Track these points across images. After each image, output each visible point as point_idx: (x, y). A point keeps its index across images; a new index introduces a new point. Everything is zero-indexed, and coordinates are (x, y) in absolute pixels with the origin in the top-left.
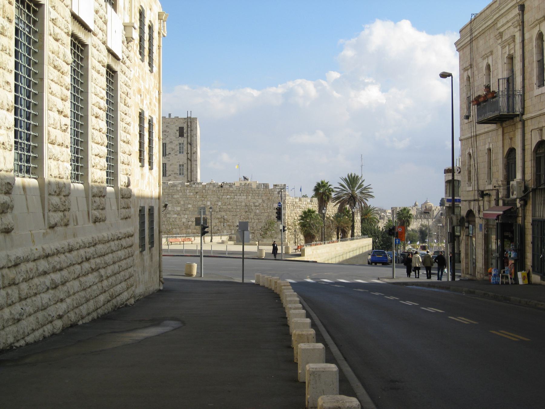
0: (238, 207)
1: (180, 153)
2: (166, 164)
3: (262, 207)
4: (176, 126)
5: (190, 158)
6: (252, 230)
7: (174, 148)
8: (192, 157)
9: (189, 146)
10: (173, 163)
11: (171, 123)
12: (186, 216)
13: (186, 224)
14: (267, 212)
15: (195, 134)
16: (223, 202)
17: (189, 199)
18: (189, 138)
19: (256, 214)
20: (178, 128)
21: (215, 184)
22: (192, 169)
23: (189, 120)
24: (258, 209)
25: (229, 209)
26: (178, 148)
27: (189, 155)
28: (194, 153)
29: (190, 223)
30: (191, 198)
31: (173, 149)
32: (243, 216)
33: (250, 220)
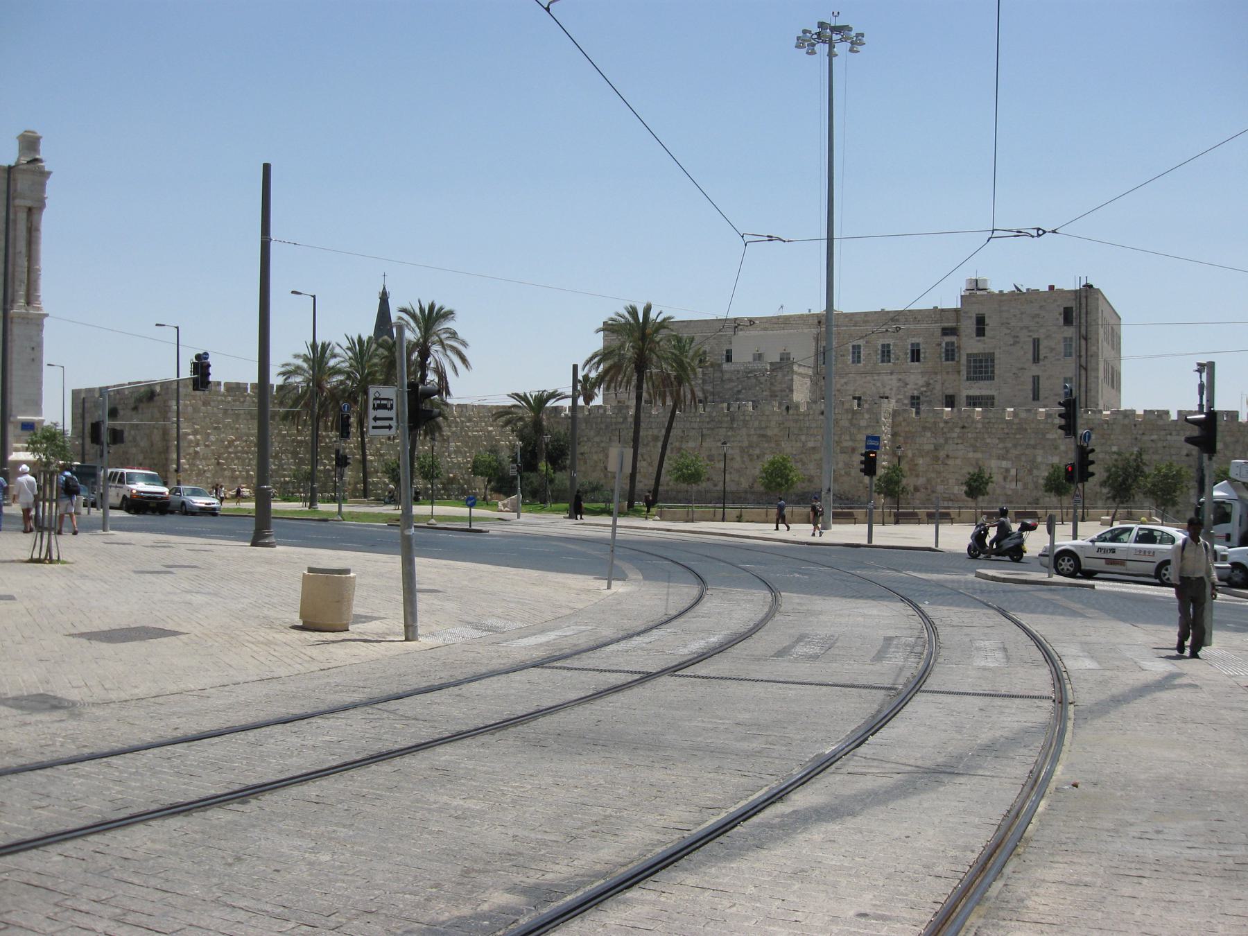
1: (1065, 356)
2: (1038, 377)
4: (1058, 306)
5: (1084, 364)
8: (1089, 365)
9: (1083, 342)
15: (1095, 320)
18: (1083, 329)
20: (1062, 309)
22: (1089, 386)
26: (1061, 347)
27: (1083, 359)
28: (1092, 356)
31: (1052, 350)
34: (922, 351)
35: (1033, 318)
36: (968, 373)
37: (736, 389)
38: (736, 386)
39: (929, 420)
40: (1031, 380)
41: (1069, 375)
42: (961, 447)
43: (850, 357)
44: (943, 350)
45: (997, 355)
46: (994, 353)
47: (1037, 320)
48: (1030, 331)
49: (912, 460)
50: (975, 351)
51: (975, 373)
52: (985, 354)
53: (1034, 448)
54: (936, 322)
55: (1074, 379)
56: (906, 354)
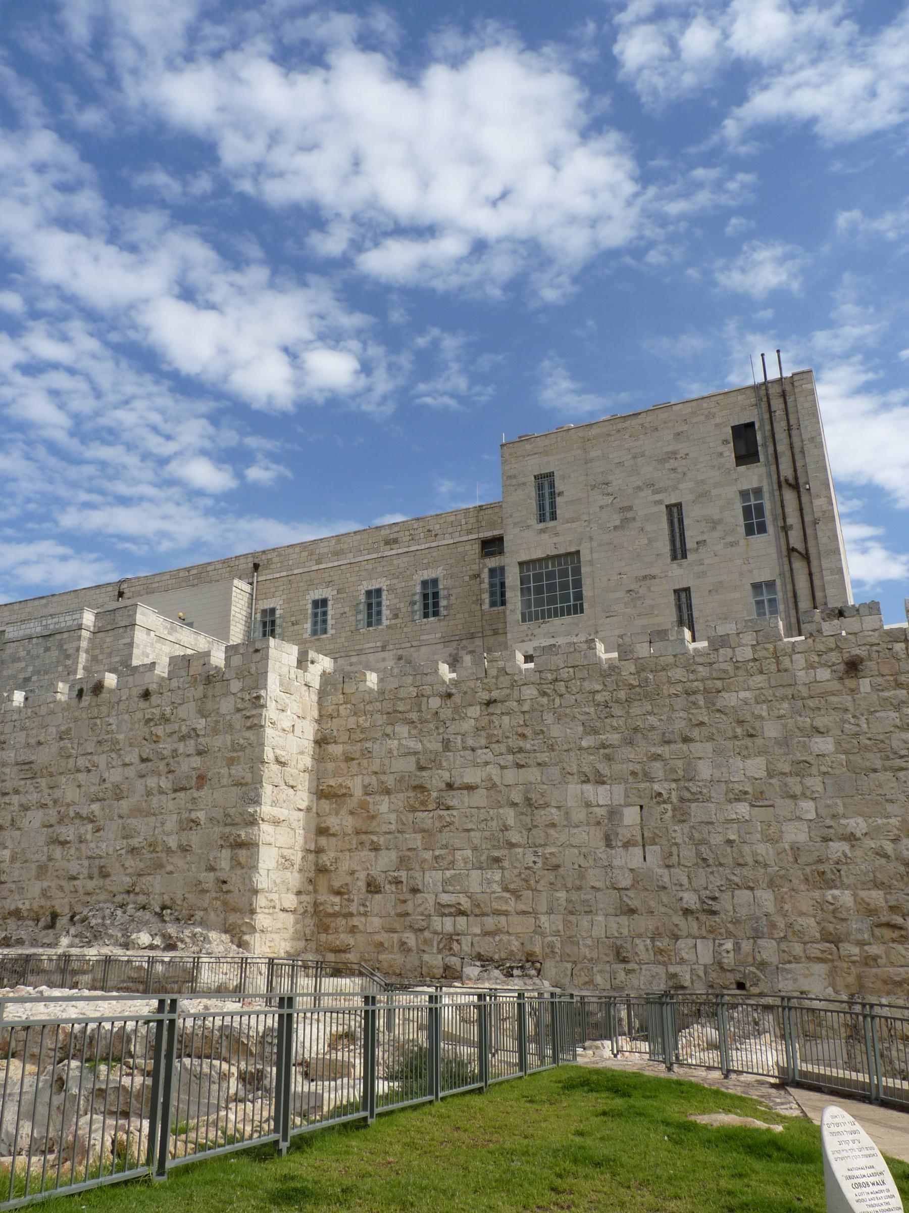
4: (717, 425)
5: (800, 546)
7: (716, 517)
8: (811, 543)
9: (789, 496)
10: (721, 582)
11: (695, 420)
12: (808, 808)
17: (811, 703)
22: (819, 595)
23: (774, 391)
29: (838, 848)
30: (822, 695)
31: (714, 524)
34: (442, 593)
35: (662, 461)
36: (527, 604)
37: (22, 676)
38: (23, 669)
39: (402, 693)
40: (672, 598)
41: (764, 576)
42: (483, 755)
43: (308, 626)
44: (486, 585)
45: (585, 556)
46: (578, 552)
47: (672, 464)
48: (657, 492)
49: (363, 805)
50: (538, 554)
51: (539, 603)
52: (559, 556)
53: (686, 740)
54: (469, 532)
56: (413, 603)
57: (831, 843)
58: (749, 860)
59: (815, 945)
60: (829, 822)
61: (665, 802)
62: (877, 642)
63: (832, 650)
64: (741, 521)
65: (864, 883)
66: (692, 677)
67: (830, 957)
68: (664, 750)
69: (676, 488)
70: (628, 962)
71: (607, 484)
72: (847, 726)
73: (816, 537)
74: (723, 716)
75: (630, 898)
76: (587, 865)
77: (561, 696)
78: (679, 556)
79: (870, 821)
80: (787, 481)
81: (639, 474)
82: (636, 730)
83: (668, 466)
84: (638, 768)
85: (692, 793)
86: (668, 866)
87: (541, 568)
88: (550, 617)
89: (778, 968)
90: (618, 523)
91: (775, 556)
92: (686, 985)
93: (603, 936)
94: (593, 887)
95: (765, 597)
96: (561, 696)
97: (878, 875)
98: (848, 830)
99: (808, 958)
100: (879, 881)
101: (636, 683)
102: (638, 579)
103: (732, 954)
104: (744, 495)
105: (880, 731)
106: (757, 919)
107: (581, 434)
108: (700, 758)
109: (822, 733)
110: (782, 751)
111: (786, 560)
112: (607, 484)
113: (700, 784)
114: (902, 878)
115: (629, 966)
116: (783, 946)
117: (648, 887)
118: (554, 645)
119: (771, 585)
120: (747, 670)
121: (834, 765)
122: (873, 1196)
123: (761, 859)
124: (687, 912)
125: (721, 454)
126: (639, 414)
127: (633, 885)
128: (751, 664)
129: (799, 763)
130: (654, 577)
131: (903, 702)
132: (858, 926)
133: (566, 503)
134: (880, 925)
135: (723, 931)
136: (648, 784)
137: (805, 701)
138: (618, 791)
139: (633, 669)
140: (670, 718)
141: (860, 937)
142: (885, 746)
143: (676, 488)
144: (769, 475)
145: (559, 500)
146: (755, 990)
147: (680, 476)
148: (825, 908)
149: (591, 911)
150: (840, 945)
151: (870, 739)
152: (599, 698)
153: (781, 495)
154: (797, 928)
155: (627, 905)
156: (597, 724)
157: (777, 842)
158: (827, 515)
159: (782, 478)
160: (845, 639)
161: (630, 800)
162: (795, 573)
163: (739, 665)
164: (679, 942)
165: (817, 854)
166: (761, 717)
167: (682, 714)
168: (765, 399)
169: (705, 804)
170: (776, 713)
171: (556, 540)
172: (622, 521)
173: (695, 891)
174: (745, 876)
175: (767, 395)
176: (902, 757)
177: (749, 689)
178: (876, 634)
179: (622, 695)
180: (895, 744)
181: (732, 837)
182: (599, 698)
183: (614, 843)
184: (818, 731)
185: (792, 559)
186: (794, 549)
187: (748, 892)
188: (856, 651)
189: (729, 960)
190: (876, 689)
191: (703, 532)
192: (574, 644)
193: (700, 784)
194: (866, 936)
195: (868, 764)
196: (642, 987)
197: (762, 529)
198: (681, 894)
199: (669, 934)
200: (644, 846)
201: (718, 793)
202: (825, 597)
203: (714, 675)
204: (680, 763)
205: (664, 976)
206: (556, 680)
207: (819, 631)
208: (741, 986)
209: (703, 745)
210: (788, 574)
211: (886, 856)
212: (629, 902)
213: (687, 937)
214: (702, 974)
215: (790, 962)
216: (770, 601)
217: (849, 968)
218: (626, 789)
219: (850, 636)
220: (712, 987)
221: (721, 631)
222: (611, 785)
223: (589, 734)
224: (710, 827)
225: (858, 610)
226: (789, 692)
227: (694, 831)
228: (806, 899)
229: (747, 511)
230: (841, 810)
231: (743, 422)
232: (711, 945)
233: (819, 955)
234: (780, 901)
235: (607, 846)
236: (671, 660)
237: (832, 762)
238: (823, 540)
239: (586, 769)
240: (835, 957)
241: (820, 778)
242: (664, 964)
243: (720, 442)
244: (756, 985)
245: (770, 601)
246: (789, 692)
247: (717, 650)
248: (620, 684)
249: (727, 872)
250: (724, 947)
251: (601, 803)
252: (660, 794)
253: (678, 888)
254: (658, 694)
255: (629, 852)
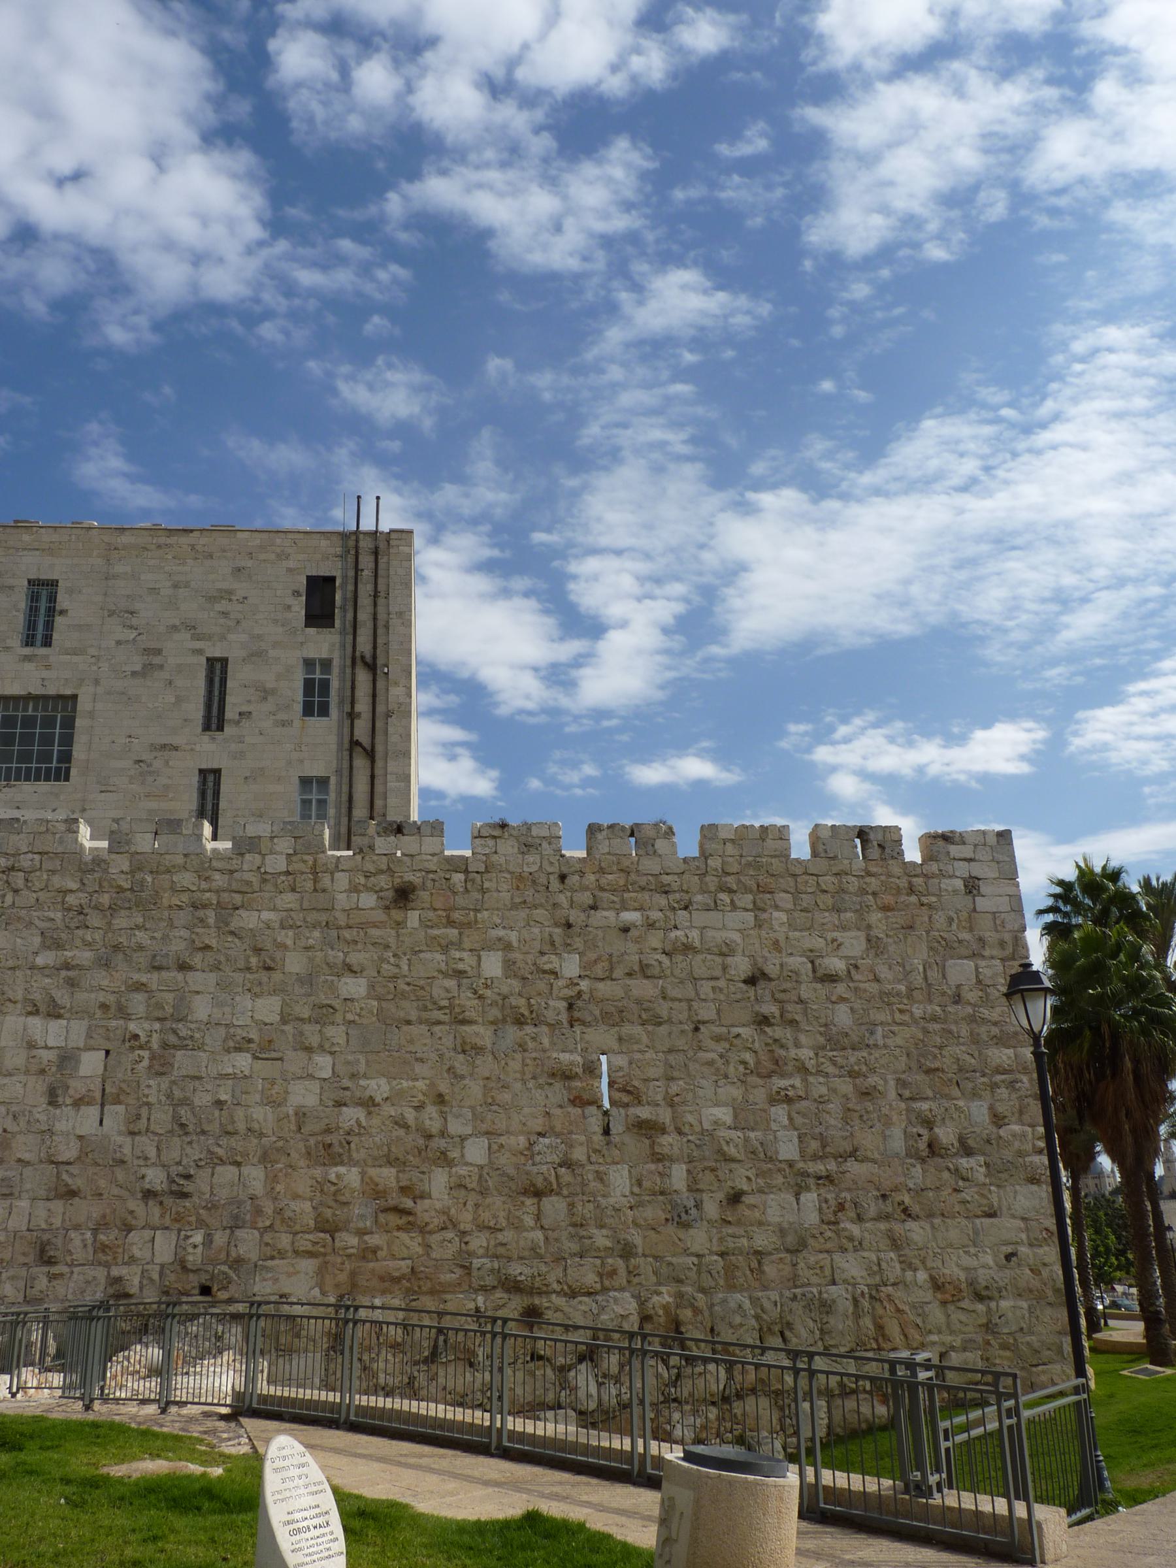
0: (706, 988)
1: (308, 710)
2: (217, 772)
3: (873, 988)
4: (290, 570)
5: (365, 740)
6: (815, 1158)
7: (270, 685)
8: (379, 738)
9: (363, 676)
11: (262, 556)
12: (323, 1064)
13: (319, 1127)
14: (906, 1018)
16: (592, 956)
17: (347, 934)
19: (834, 1041)
21: (534, 832)
22: (378, 803)
23: (366, 544)
24: (842, 999)
25: (638, 1002)
29: (352, 1115)
30: (362, 926)
31: (265, 693)
32: (748, 1057)
33: (797, 1082)
35: (212, 599)
40: (195, 779)
45: (83, 704)
46: (74, 697)
47: (222, 606)
48: (197, 637)
52: (45, 698)
53: (184, 967)
55: (333, 780)
57: (344, 1109)
58: (241, 1126)
59: (307, 1236)
60: (346, 1082)
61: (141, 1047)
62: (434, 868)
63: (382, 872)
64: (300, 697)
65: (375, 1159)
66: (204, 885)
67: (322, 1250)
68: (152, 979)
69: (223, 638)
70: (56, 1263)
71: (132, 613)
72: (385, 966)
73: (386, 733)
74: (237, 940)
75: (72, 1175)
76: (16, 1129)
77: (16, 891)
78: (214, 726)
79: (395, 1083)
80: (363, 657)
81: (178, 609)
82: (116, 948)
83: (218, 607)
84: (111, 999)
85: (179, 1037)
86: (132, 1133)
87: (16, 709)
88: (18, 779)
89: (256, 1266)
90: (138, 668)
91: (334, 747)
92: (132, 1292)
93: (25, 1228)
94: (19, 1160)
95: (314, 797)
96: (16, 891)
97: (393, 1149)
98: (367, 1094)
99: (296, 1252)
100: (392, 1157)
101: (127, 886)
102: (154, 747)
103: (200, 1250)
104: (309, 664)
105: (422, 975)
106: (240, 1204)
107: (106, 539)
108: (198, 993)
109: (355, 972)
110: (303, 991)
111: (346, 754)
112: (132, 613)
113: (193, 1026)
114: (420, 1153)
115: (55, 1270)
116: (267, 1238)
117: (100, 1161)
118: (18, 820)
119: (323, 782)
120: (276, 885)
121: (363, 1013)
122: (313, 1542)
123: (256, 1126)
124: (149, 1194)
125: (289, 607)
126: (192, 531)
127: (79, 1158)
128: (283, 878)
129: (322, 1007)
130: (176, 749)
131: (452, 943)
132: (360, 1211)
133: (69, 626)
134: (386, 1210)
135: (193, 1219)
136: (121, 1022)
137: (341, 932)
138: (78, 1028)
139: (126, 868)
140: (165, 937)
141: (361, 1225)
142: (424, 993)
143: (223, 638)
144: (343, 646)
145: (59, 620)
146: (223, 1295)
147: (232, 623)
148: (325, 1189)
149: (11, 1194)
150: (337, 1234)
151: (408, 984)
152: (71, 899)
153: (353, 674)
154: (288, 1214)
155: (67, 1185)
156: (63, 935)
157: (279, 1105)
158: (402, 708)
159: (358, 654)
160: (399, 860)
161: (92, 1042)
162: (355, 772)
163: (268, 877)
164: (132, 1234)
165: (326, 1121)
166: (284, 947)
167: (184, 933)
168: (353, 552)
169: (195, 1053)
170: (303, 943)
171: (45, 674)
172: (145, 666)
173: (164, 1166)
174: (232, 1148)
175: (357, 548)
176: (440, 1008)
177: (274, 909)
178: (435, 859)
179: (105, 899)
180: (437, 992)
181: (223, 1097)
182: (71, 899)
183: (60, 1100)
184: (350, 969)
185: (354, 755)
186: (358, 743)
187: (234, 1170)
188: (410, 877)
189: (194, 1257)
190: (425, 924)
191: (249, 701)
192: (48, 821)
193: (193, 1026)
194: (368, 1223)
195: (402, 1014)
196: (70, 1297)
197: (324, 711)
198: (143, 1170)
199: (118, 1223)
200: (103, 1105)
201: (215, 1039)
202: (385, 806)
203: (234, 886)
204: (169, 997)
205: (103, 1281)
206: (12, 869)
207: (371, 847)
208: (205, 1290)
209: (204, 975)
210: (346, 773)
211: (406, 1127)
212: (70, 1181)
213: (143, 1228)
214: (156, 1276)
215: (272, 1258)
216: (320, 802)
217: (343, 1264)
218: (90, 1027)
219: (405, 858)
220: (167, 1293)
221: (251, 831)
222: (69, 1020)
223: (49, 948)
224: (197, 1082)
225: (419, 828)
226: (323, 917)
227: (174, 1087)
228: (303, 1179)
229: (309, 685)
230: (362, 1068)
231: (322, 574)
232: (174, 1237)
233: (310, 1247)
234: (272, 1179)
235: (50, 1103)
236: (180, 860)
237: (361, 1009)
238: (393, 738)
239: (37, 996)
240: (329, 1250)
241: (344, 1028)
242: (107, 1265)
243: (290, 592)
244: (225, 1288)
245: (320, 802)
246: (323, 917)
247: (242, 855)
248: (105, 884)
249: (210, 1142)
250: (191, 1240)
251: (50, 1045)
252: (136, 1037)
253: (142, 1162)
254: (155, 904)
255: (81, 1113)
